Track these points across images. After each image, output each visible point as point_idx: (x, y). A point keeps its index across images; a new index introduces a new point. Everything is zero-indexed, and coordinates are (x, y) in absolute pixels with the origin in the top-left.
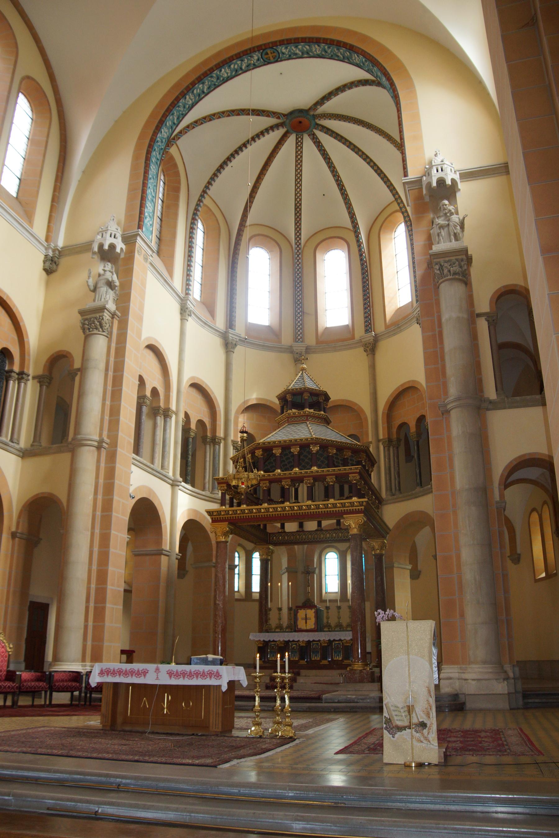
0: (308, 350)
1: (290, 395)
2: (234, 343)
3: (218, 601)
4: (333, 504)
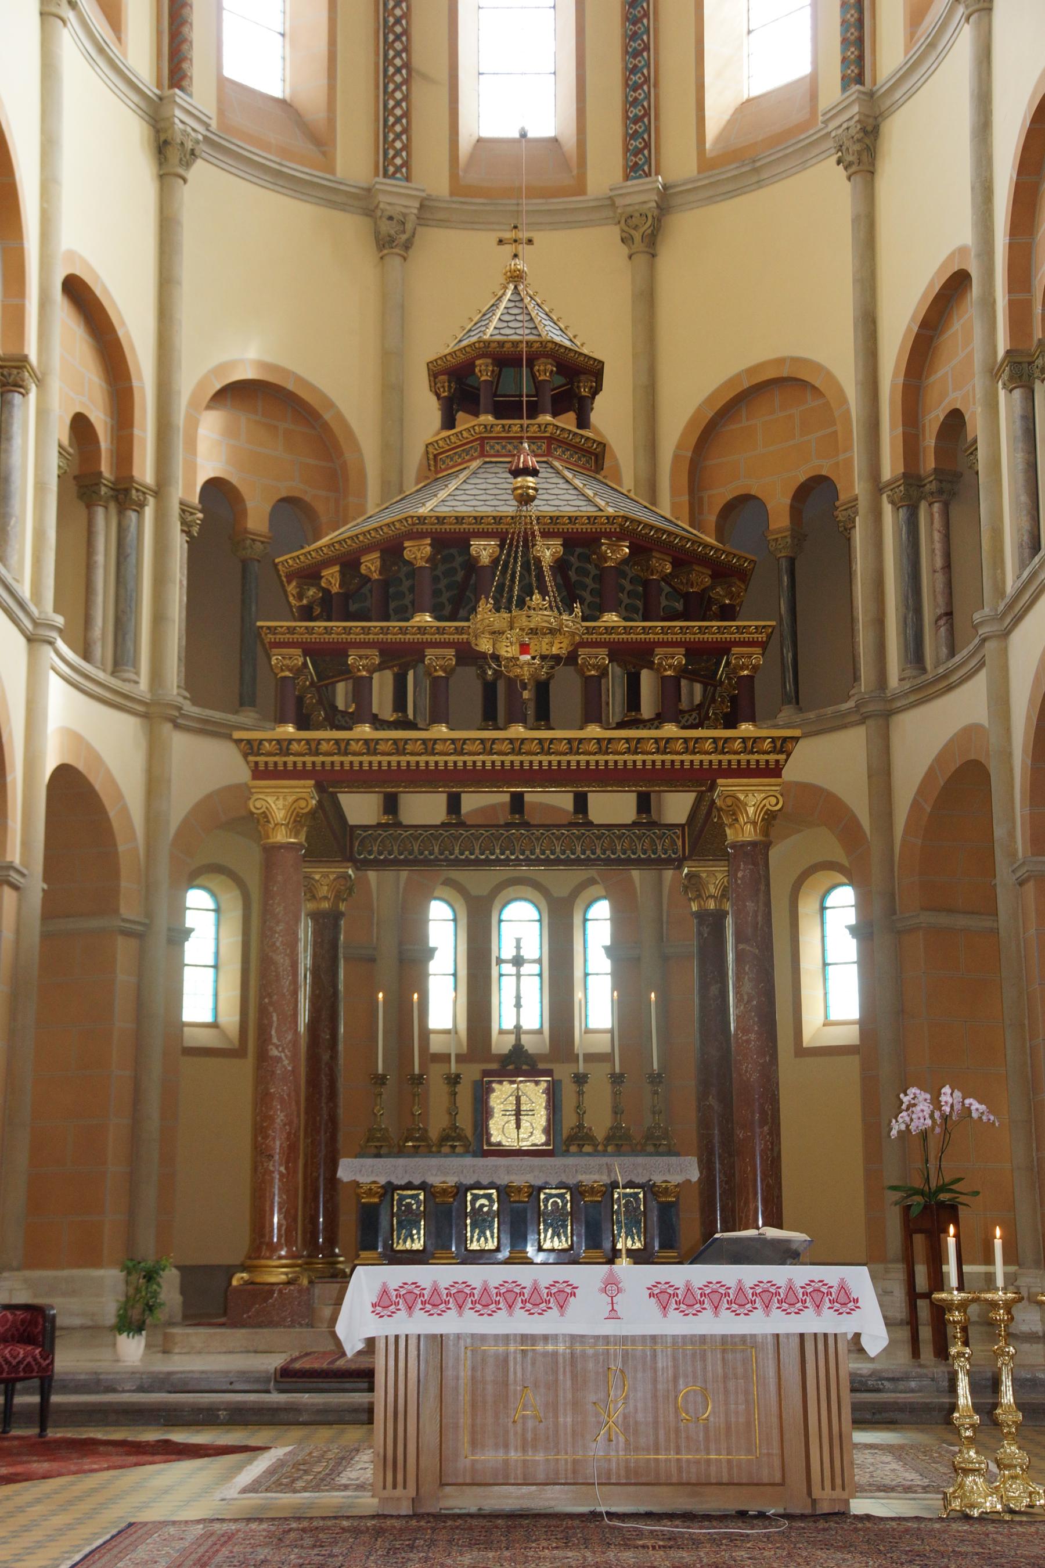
1: (489, 361)
2: (189, 145)
3: (277, 1047)
4: (366, 742)
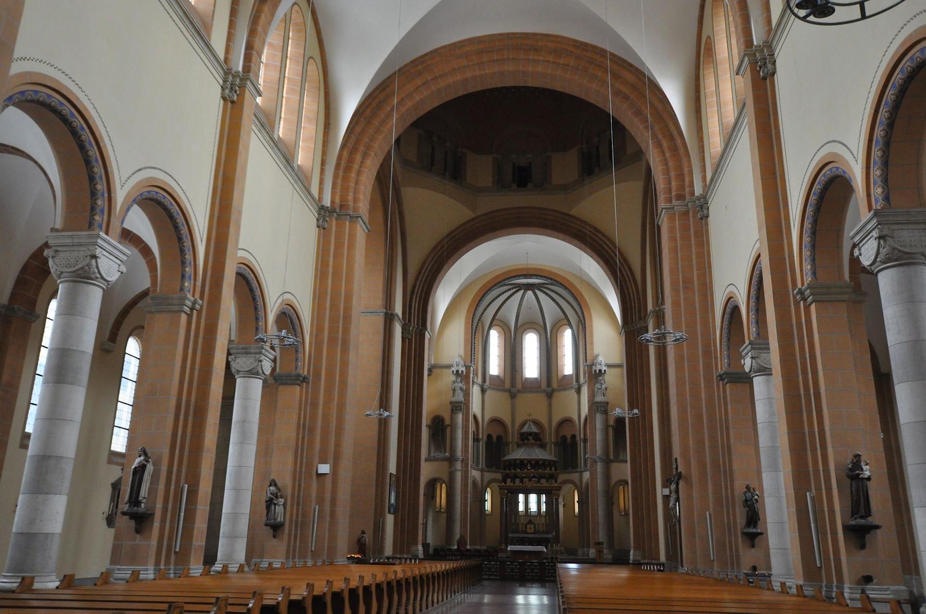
0: (519, 391)
